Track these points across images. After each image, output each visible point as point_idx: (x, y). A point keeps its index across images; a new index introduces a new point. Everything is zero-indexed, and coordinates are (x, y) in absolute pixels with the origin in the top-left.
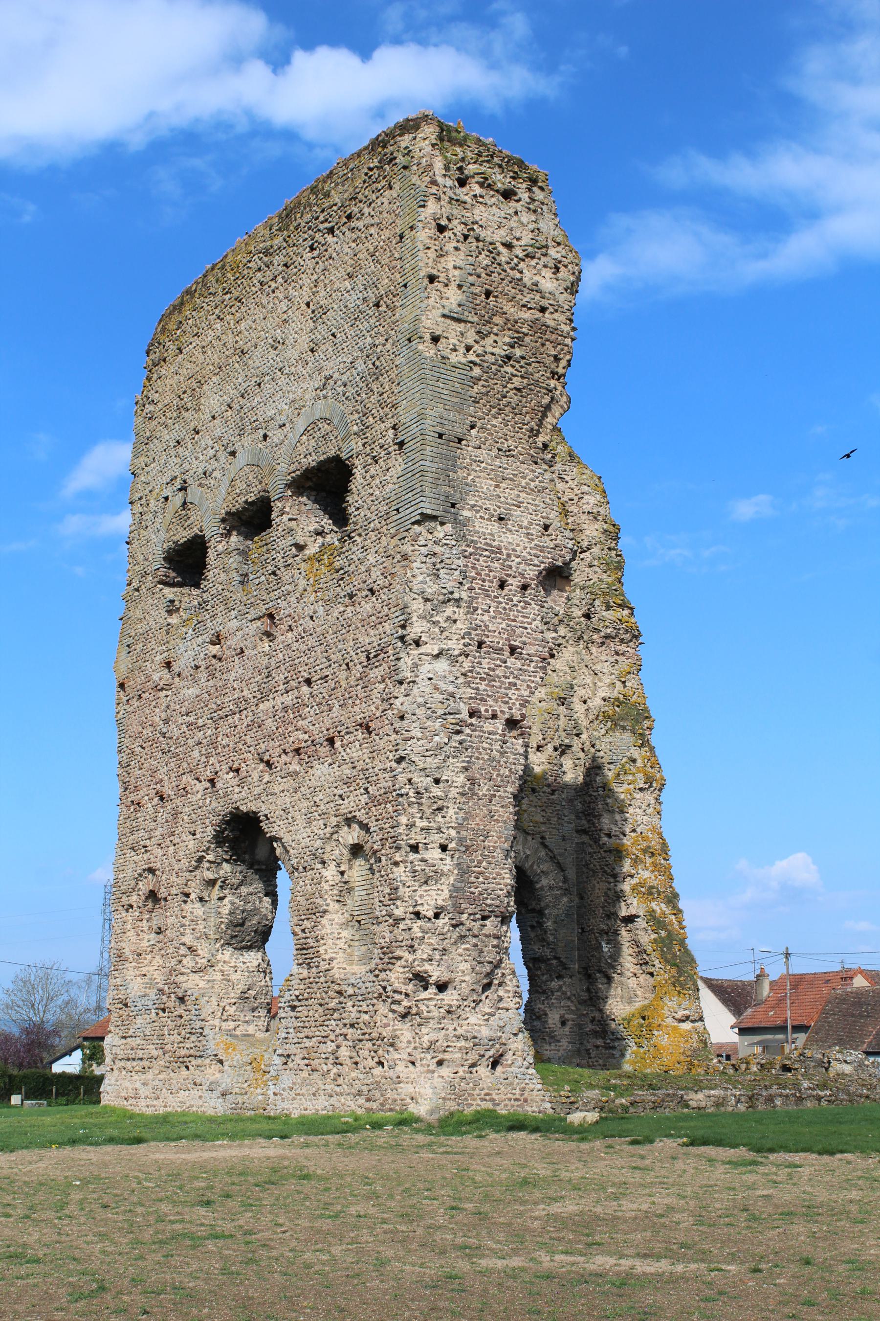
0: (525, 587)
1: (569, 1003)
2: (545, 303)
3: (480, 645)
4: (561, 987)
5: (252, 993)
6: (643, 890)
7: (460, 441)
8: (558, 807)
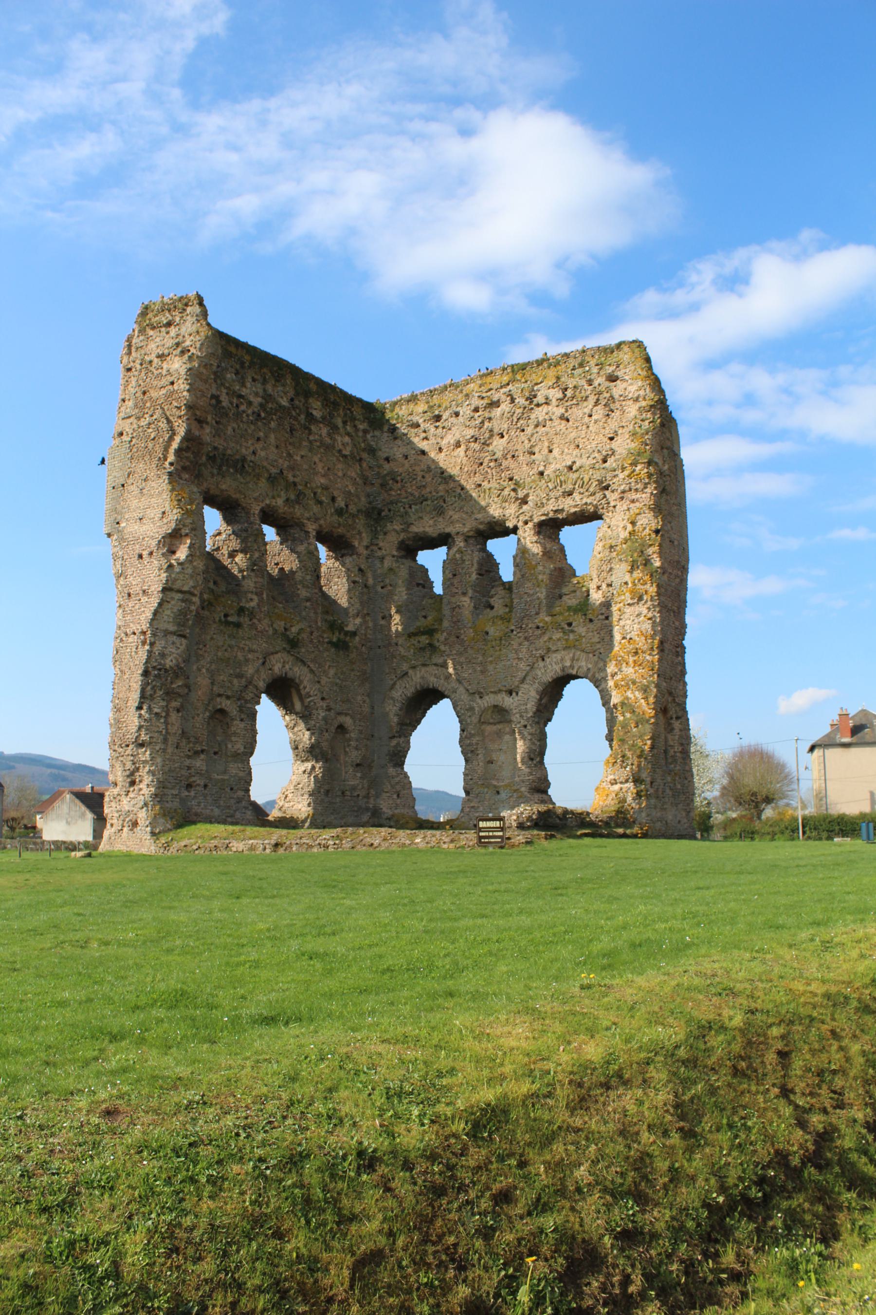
0: (151, 554)
2: (171, 379)
3: (129, 595)
7: (123, 485)
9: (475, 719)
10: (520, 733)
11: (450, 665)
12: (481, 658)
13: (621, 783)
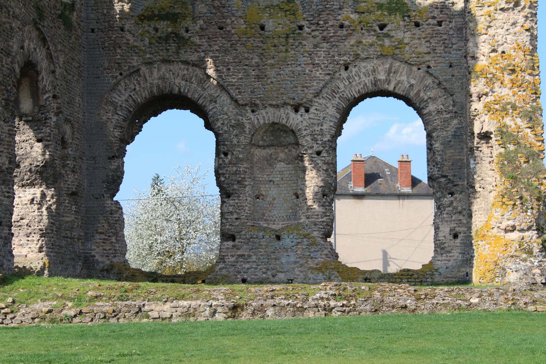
1: (461, 217)
4: (452, 202)
5: (25, 221)
6: (497, 107)
8: (445, 37)
9: (244, 140)
10: (312, 160)
11: (210, 63)
12: (256, 60)
13: (522, 230)
